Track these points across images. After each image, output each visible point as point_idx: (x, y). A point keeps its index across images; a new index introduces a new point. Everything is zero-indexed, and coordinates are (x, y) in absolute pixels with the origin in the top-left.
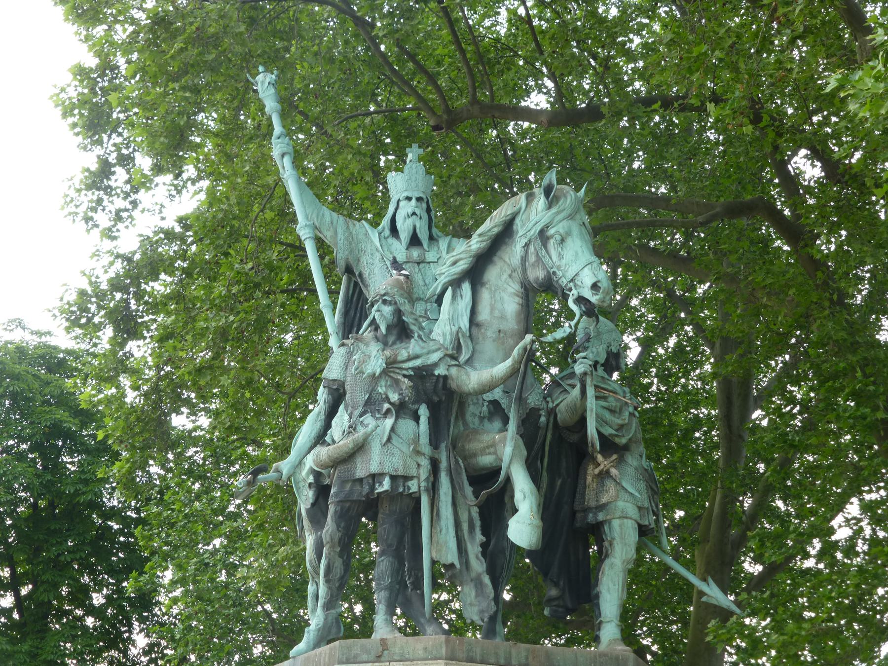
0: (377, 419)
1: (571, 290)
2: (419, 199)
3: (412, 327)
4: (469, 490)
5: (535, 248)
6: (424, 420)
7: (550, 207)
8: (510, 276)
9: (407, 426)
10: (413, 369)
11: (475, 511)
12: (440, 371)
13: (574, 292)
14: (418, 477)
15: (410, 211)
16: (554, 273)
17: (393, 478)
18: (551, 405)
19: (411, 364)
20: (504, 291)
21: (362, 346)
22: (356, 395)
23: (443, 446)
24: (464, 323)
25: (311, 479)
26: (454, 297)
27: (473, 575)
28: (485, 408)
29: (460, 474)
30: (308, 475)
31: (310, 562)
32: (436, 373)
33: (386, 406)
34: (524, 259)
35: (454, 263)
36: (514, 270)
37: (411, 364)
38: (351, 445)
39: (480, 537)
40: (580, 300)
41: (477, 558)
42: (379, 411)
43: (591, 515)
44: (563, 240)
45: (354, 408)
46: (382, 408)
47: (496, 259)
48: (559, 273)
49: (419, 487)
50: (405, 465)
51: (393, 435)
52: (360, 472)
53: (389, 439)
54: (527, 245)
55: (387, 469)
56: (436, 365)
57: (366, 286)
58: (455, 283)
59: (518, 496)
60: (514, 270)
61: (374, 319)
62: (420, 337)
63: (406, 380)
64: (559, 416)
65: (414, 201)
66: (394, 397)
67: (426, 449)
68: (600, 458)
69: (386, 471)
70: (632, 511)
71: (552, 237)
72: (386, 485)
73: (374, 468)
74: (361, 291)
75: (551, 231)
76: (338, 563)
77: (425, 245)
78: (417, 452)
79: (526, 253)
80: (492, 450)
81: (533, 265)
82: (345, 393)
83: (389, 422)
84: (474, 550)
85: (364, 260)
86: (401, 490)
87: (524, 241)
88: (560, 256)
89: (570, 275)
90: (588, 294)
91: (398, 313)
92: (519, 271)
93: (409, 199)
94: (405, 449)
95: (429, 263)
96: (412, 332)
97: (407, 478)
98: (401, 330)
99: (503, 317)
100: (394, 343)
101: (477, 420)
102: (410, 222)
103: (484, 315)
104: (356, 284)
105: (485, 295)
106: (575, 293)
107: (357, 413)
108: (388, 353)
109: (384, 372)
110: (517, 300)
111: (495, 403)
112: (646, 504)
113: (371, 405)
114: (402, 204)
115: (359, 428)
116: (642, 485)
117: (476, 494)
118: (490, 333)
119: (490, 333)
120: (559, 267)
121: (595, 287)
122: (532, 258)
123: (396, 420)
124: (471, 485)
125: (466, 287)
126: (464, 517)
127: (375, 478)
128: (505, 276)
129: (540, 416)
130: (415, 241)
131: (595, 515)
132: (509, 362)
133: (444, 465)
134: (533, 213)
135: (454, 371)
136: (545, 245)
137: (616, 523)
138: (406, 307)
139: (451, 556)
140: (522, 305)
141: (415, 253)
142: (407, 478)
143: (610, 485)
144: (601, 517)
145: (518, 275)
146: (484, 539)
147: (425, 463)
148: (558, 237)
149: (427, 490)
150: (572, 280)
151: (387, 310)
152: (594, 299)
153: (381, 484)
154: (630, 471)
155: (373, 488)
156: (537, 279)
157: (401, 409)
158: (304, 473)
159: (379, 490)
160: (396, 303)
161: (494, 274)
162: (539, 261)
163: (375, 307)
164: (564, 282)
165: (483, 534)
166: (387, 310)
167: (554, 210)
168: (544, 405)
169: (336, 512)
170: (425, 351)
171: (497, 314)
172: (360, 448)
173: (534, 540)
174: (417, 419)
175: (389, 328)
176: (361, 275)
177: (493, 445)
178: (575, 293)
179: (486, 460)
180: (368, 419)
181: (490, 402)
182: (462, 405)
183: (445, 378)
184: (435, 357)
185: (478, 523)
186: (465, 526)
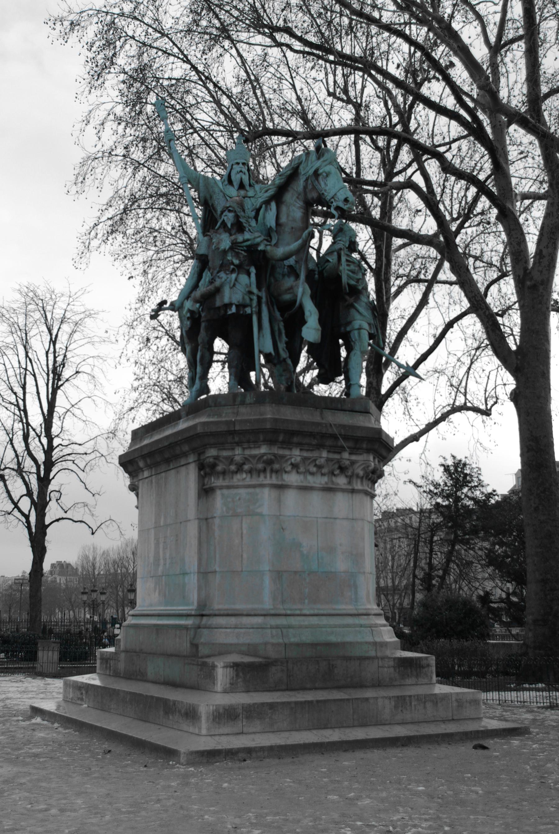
0: (227, 274)
1: (332, 203)
2: (244, 164)
3: (245, 225)
4: (278, 314)
6: (253, 276)
7: (319, 158)
8: (298, 198)
9: (243, 278)
10: (246, 246)
11: (282, 325)
12: (261, 248)
14: (251, 306)
15: (239, 170)
16: (323, 194)
17: (236, 306)
18: (320, 269)
19: (245, 244)
20: (294, 206)
21: (218, 235)
22: (215, 262)
23: (264, 289)
24: (273, 224)
25: (188, 315)
26: (266, 210)
27: (282, 359)
28: (286, 270)
29: (273, 307)
30: (187, 313)
32: (259, 248)
33: (232, 267)
34: (305, 188)
35: (266, 191)
36: (299, 194)
37: (245, 244)
38: (213, 289)
39: (284, 338)
40: (338, 208)
41: (283, 350)
42: (228, 270)
43: (343, 329)
44: (327, 176)
45: (214, 269)
47: (289, 189)
48: (326, 194)
49: (252, 311)
50: (243, 298)
51: (237, 284)
52: (218, 303)
53: (234, 285)
54: (307, 180)
55: (234, 301)
56: (258, 244)
58: (267, 203)
59: (307, 313)
60: (299, 194)
61: (224, 220)
62: (249, 230)
63: (243, 252)
64: (325, 274)
65: (241, 165)
66: (236, 262)
67: (255, 290)
68: (347, 297)
69: (233, 302)
70: (366, 326)
71: (321, 174)
72: (234, 309)
73: (226, 300)
74: (213, 214)
75: (320, 171)
77: (247, 187)
78: (250, 293)
79: (307, 184)
80: (291, 291)
82: (208, 262)
83: (234, 276)
84: (282, 346)
85: (214, 197)
86: (241, 312)
87: (304, 179)
88: (326, 185)
89: (331, 194)
90: (341, 205)
91: (237, 217)
92: (303, 194)
93: (238, 164)
94: (243, 290)
95: (250, 197)
96: (245, 227)
97: (245, 306)
98: (239, 227)
99: (294, 220)
100: (235, 234)
101: (281, 277)
102: (239, 176)
103: (283, 219)
104: (210, 211)
105: (284, 209)
106: (335, 204)
107: (216, 272)
108: (233, 237)
109: (231, 248)
110: (302, 210)
111: (290, 267)
112: (372, 322)
113: (223, 267)
114: (234, 166)
116: (370, 312)
117: (282, 315)
118: (287, 229)
119: (286, 229)
120: (325, 191)
121: (346, 200)
122: (310, 187)
123: (238, 274)
124: (279, 311)
125: (273, 205)
126: (276, 328)
127: (228, 306)
128: (295, 198)
129: (315, 274)
130: (242, 186)
131: (345, 328)
132: (300, 241)
133: (264, 300)
134: (309, 162)
135: (269, 248)
136: (317, 179)
137: (356, 332)
138: (241, 214)
139: (269, 348)
140: (304, 213)
141: (242, 192)
142: (245, 306)
143: (353, 311)
144: (348, 329)
145: (302, 197)
146: (287, 340)
147: (255, 298)
148: (324, 174)
149: (256, 313)
150: (333, 198)
151: (231, 215)
152: (345, 207)
153: (231, 310)
154: (364, 304)
155: (226, 312)
156: (313, 198)
157: (240, 268)
158: (184, 312)
159: (230, 312)
160: (235, 212)
161: (289, 197)
162: (314, 188)
163: (224, 214)
164: (328, 198)
165: (287, 337)
166: (231, 215)
167: (322, 160)
168: (317, 269)
170: (253, 237)
171: (290, 218)
172: (218, 290)
173: (317, 338)
174: (249, 274)
175: (232, 225)
176: (213, 205)
177: (291, 288)
178: (335, 204)
179: (287, 297)
180: (222, 274)
181: (288, 266)
182: (273, 268)
183: (264, 252)
184: (258, 240)
185: (283, 331)
186: (277, 334)
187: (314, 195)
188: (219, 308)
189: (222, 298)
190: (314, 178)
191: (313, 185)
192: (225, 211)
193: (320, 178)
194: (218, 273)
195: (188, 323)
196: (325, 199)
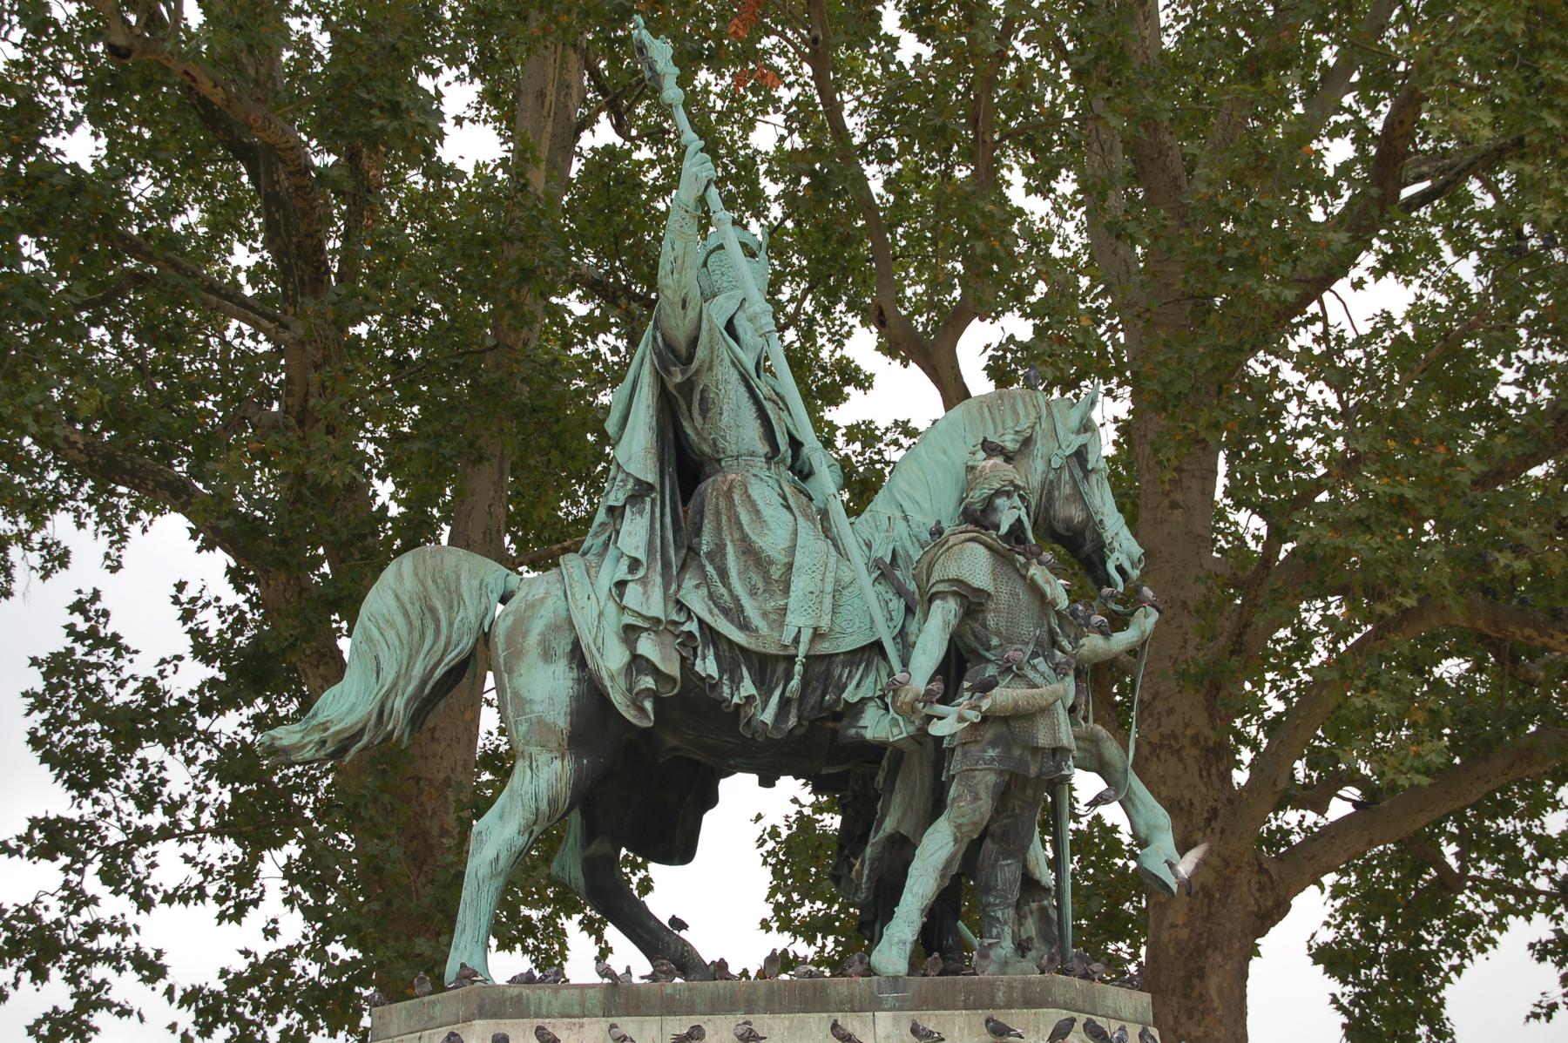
1: (1112, 550)
5: (1072, 476)
13: (1116, 554)
25: (648, 682)
31: (553, 801)
34: (1049, 488)
40: (1120, 569)
46: (1053, 656)
52: (1043, 739)
57: (704, 412)
73: (1065, 743)
76: (959, 856)
81: (1067, 498)
90: (1127, 566)
115: (1031, 674)
156: (1068, 521)
162: (1079, 496)
164: (1107, 536)
169: (996, 785)
187: (1077, 515)
188: (1036, 750)
189: (1054, 728)
190: (1079, 474)
191: (1075, 486)
192: (1009, 495)
193: (1093, 478)
194: (1035, 655)
195: (648, 705)
196: (1100, 535)
